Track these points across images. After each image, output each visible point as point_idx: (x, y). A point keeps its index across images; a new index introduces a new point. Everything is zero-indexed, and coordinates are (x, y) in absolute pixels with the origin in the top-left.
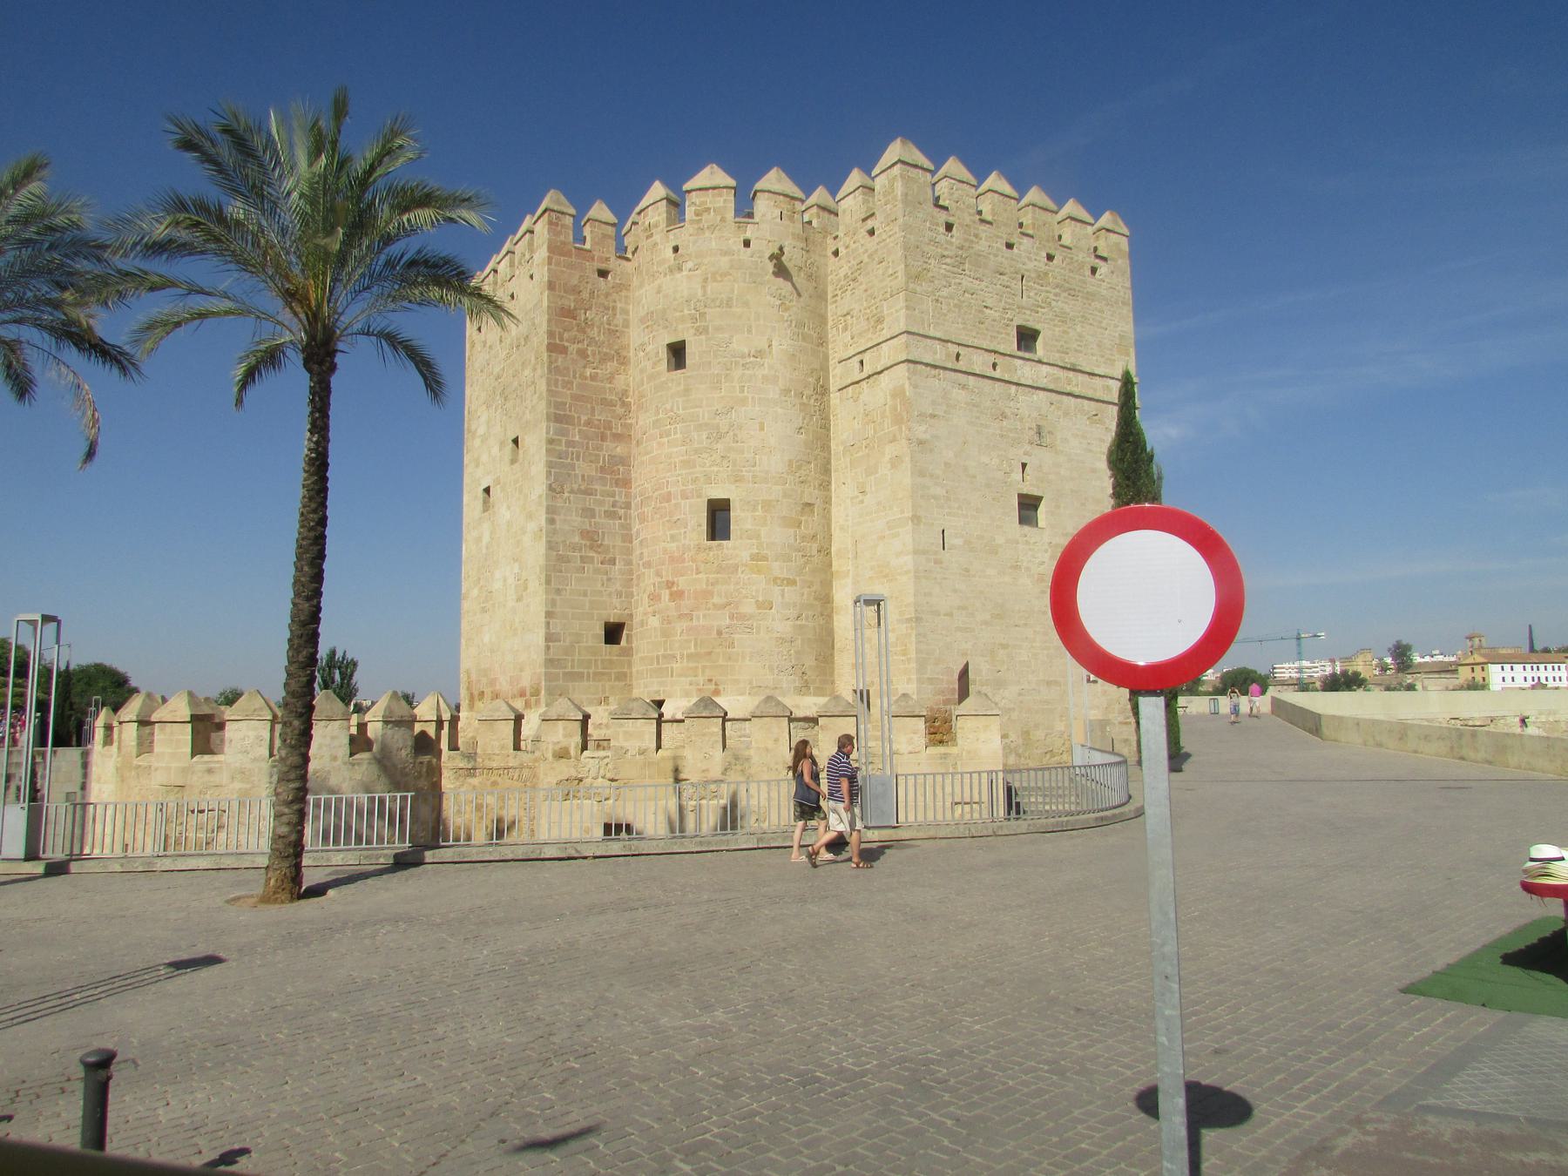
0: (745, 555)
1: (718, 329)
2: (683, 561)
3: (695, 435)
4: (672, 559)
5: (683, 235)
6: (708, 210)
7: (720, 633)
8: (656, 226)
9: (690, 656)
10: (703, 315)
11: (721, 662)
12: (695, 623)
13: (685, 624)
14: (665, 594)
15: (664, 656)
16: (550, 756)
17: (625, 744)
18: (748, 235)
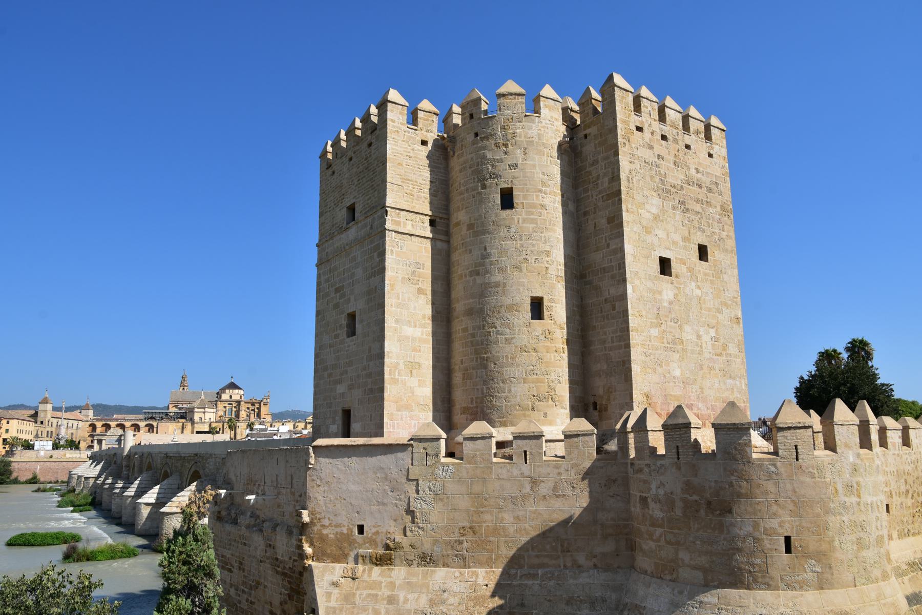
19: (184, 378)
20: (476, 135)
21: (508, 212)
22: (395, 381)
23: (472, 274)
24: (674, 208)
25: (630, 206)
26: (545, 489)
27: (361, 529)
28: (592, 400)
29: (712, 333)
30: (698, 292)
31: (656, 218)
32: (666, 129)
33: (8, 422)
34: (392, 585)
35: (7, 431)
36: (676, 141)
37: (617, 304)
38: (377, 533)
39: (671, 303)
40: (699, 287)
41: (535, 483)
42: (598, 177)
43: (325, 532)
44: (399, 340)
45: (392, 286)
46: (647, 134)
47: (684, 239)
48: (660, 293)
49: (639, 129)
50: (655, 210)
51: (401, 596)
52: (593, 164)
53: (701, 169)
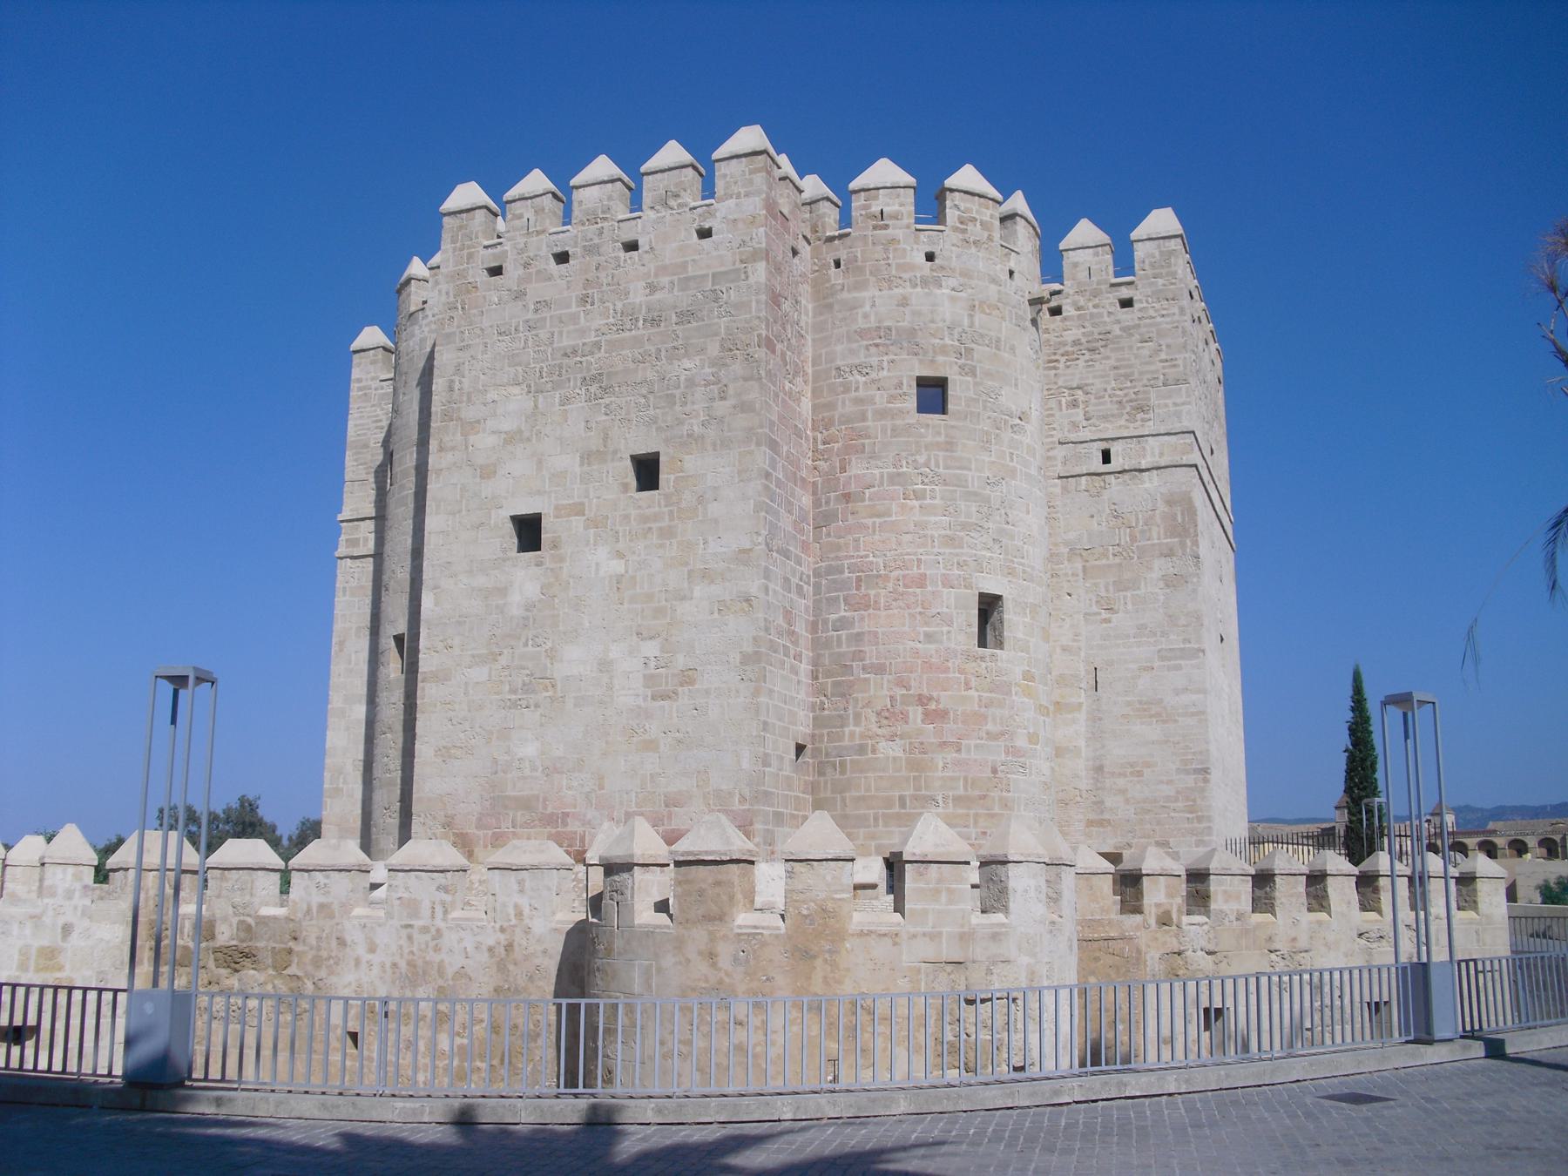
0: (1018, 672)
1: (988, 374)
2: (947, 670)
3: (962, 505)
4: (928, 666)
5: (945, 241)
6: (974, 220)
7: (994, 771)
8: (895, 217)
9: (957, 800)
10: (969, 351)
11: (997, 810)
12: (964, 755)
13: (952, 756)
14: (915, 713)
15: (915, 798)
16: (1152, 922)
17: (1225, 907)
18: (1012, 265)
22: (338, 791)
24: (566, 401)
25: (446, 439)
29: (651, 649)
30: (617, 566)
31: (511, 438)
32: (569, 238)
36: (592, 250)
39: (529, 607)
40: (620, 555)
44: (347, 729)
45: (341, 643)
46: (512, 272)
47: (587, 457)
48: (502, 591)
49: (496, 271)
50: (507, 425)
53: (665, 280)
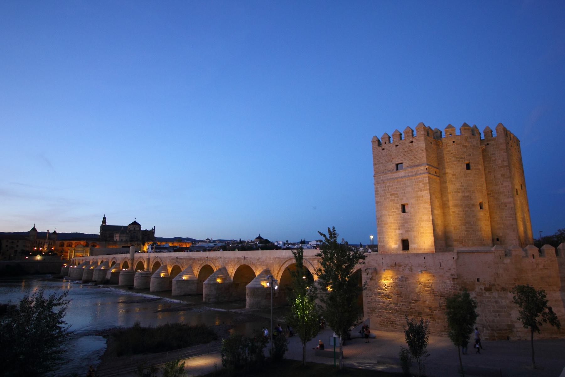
19: (105, 218)
20: (454, 142)
21: (469, 171)
23: (455, 192)
26: (540, 267)
27: (478, 280)
28: (496, 237)
33: (18, 242)
34: (494, 298)
35: (17, 246)
37: (508, 205)
38: (485, 281)
41: (537, 264)
42: (496, 159)
43: (465, 281)
51: (500, 300)
52: (493, 154)
